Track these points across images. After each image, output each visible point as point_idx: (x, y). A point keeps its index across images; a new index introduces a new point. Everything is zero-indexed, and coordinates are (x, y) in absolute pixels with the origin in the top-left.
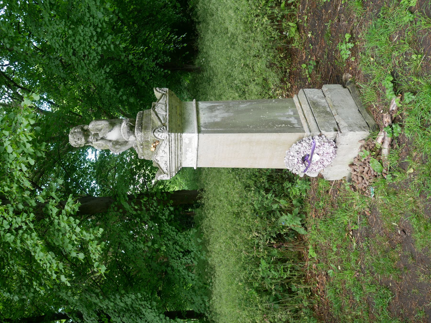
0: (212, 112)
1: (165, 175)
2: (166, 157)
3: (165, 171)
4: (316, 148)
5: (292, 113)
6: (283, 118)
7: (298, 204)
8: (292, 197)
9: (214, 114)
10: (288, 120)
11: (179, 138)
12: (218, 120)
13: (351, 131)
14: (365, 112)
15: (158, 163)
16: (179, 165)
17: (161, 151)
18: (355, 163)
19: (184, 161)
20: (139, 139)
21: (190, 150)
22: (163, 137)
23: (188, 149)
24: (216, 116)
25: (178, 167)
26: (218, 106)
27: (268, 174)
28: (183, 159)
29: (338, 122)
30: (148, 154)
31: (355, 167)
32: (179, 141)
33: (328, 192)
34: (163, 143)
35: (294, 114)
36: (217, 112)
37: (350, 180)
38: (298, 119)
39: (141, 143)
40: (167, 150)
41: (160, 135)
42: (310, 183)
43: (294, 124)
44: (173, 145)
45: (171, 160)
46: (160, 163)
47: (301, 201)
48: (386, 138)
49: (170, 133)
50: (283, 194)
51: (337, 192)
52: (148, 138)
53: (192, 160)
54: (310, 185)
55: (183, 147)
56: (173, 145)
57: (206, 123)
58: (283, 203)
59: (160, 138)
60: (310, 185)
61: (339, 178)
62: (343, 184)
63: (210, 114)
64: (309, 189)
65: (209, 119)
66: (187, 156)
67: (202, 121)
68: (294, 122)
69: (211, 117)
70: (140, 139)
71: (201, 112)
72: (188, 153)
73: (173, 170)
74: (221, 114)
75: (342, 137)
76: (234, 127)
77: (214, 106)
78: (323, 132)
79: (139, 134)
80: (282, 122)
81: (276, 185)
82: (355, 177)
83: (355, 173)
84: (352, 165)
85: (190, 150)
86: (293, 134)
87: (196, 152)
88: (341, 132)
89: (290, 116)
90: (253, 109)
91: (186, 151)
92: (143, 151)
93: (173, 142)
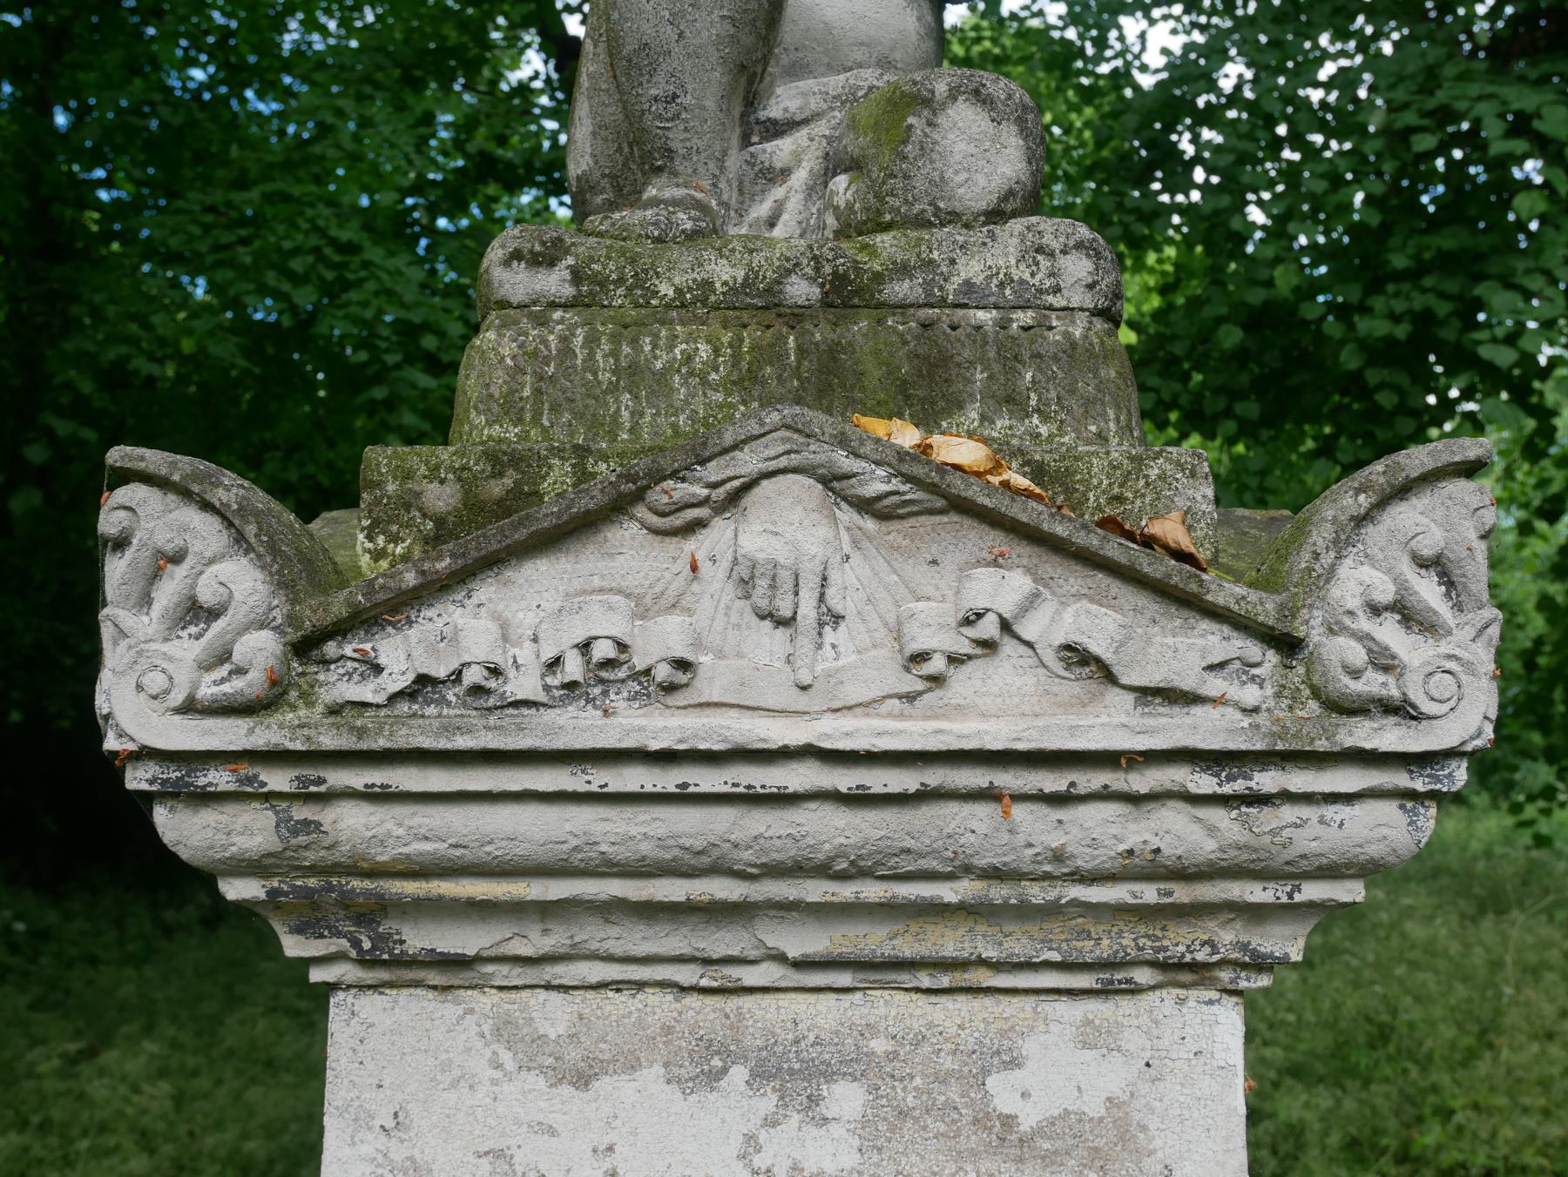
1: (261, 649)
2: (755, 688)
3: (401, 654)
11: (1180, 941)
15: (626, 535)
16: (418, 938)
17: (1003, 587)
19: (504, 1030)
20: (994, 257)
22: (1389, 632)
23: (846, 1099)
25: (371, 912)
28: (552, 1015)
30: (632, 375)
32: (1128, 940)
34: (1216, 641)
39: (901, 289)
40: (1002, 705)
44: (1099, 831)
45: (708, 780)
46: (629, 554)
49: (1460, 774)
52: (1013, 401)
55: (890, 1011)
56: (1099, 831)
59: (1359, 579)
66: (641, 1096)
70: (971, 269)
72: (738, 1103)
73: (352, 825)
79: (1078, 268)
91: (795, 1077)
92: (698, 302)
93: (1179, 832)
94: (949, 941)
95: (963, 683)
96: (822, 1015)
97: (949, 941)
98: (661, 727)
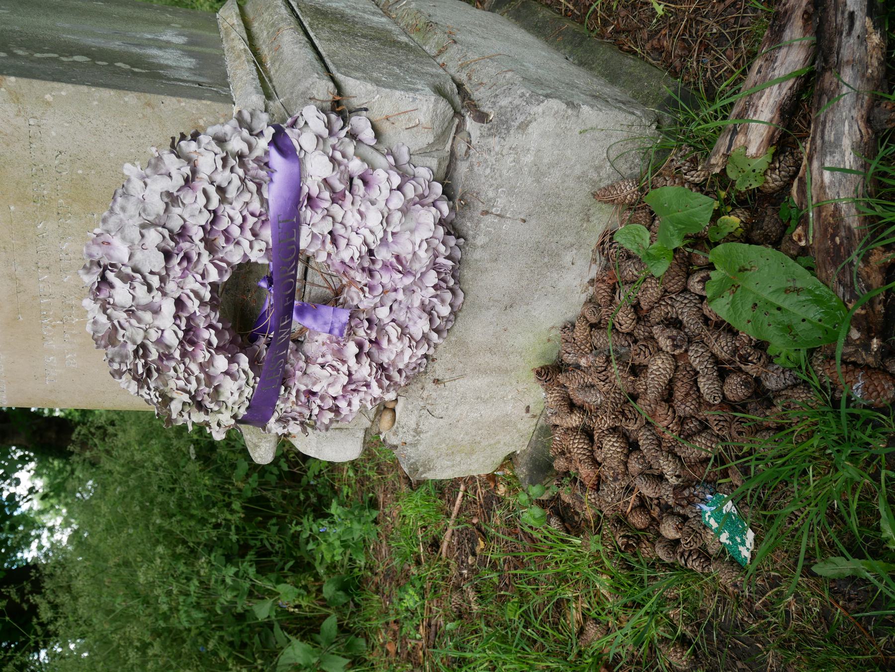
4: (307, 213)
7: (342, 598)
8: (321, 571)
13: (547, 96)
14: (605, 53)
18: (570, 359)
27: (249, 494)
29: (463, 77)
31: (572, 383)
33: (435, 544)
37: (542, 468)
42: (375, 514)
47: (353, 585)
48: (849, 47)
50: (291, 563)
51: (474, 542)
54: (376, 522)
58: (288, 594)
60: (376, 522)
61: (480, 465)
62: (500, 500)
64: (373, 536)
75: (493, 142)
78: (357, 89)
80: (71, 49)
81: (275, 529)
82: (578, 446)
83: (575, 420)
84: (551, 372)
86: (131, 98)
88: (482, 117)
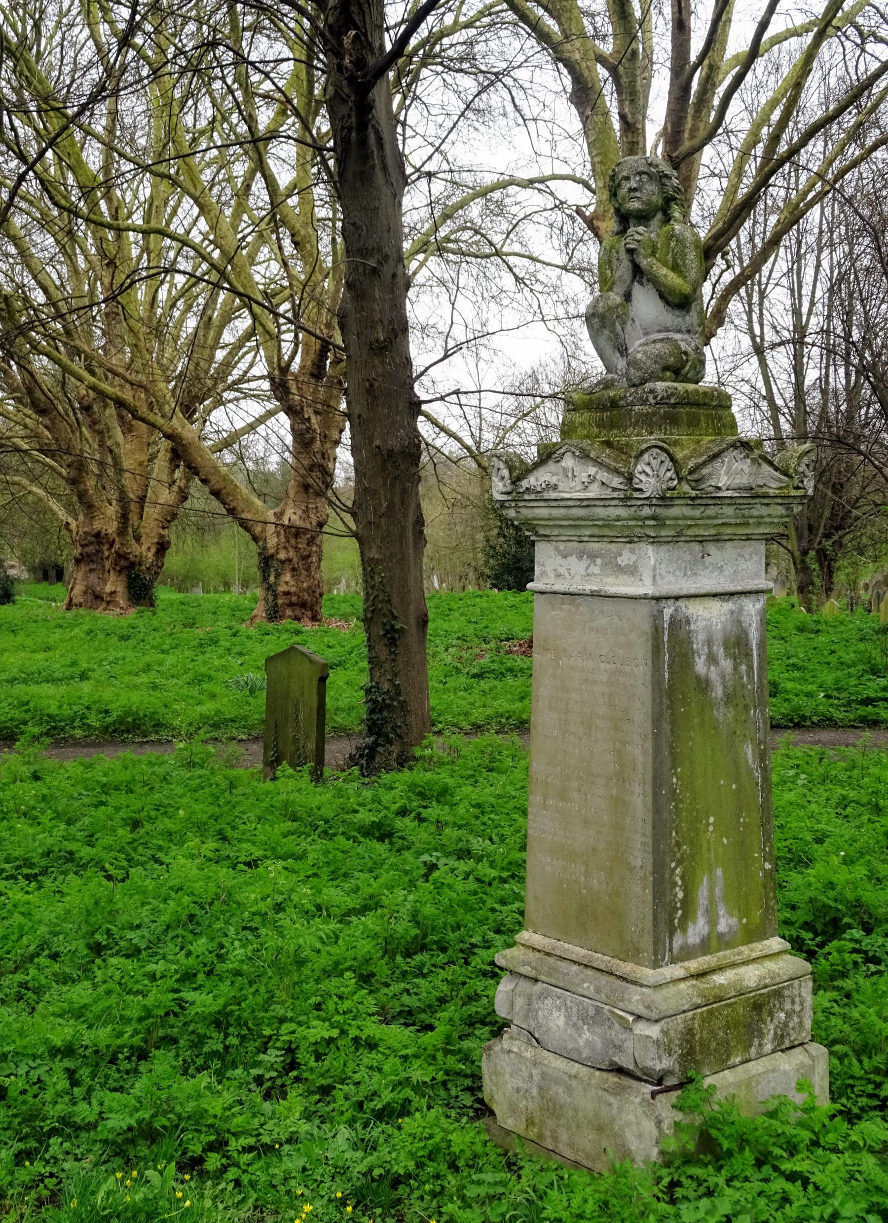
0: (726, 645)
5: (722, 926)
6: (706, 893)
9: (721, 652)
10: (700, 913)
12: (700, 666)
15: (551, 463)
16: (542, 531)
19: (557, 549)
21: (596, 570)
22: (643, 477)
23: (599, 561)
24: (712, 659)
26: (750, 667)
28: (562, 546)
35: (721, 936)
36: (726, 664)
38: (705, 947)
39: (622, 403)
40: (594, 491)
41: (648, 469)
43: (684, 931)
45: (562, 504)
53: (558, 576)
57: (688, 622)
63: (719, 637)
65: (702, 637)
66: (573, 559)
67: (694, 609)
68: (690, 931)
69: (709, 642)
71: (728, 606)
72: (585, 562)
73: (525, 512)
74: (723, 677)
76: (673, 723)
77: (748, 655)
85: (596, 570)
87: (588, 588)
89: (713, 922)
90: (738, 790)
91: (592, 557)
94: (606, 532)
95: (591, 487)
96: (594, 546)
97: (606, 532)
98: (553, 495)
